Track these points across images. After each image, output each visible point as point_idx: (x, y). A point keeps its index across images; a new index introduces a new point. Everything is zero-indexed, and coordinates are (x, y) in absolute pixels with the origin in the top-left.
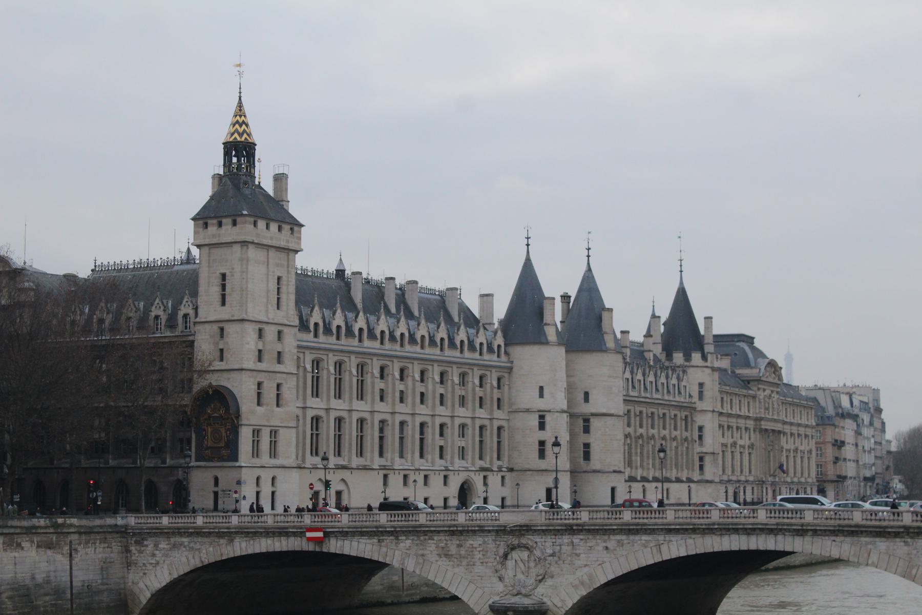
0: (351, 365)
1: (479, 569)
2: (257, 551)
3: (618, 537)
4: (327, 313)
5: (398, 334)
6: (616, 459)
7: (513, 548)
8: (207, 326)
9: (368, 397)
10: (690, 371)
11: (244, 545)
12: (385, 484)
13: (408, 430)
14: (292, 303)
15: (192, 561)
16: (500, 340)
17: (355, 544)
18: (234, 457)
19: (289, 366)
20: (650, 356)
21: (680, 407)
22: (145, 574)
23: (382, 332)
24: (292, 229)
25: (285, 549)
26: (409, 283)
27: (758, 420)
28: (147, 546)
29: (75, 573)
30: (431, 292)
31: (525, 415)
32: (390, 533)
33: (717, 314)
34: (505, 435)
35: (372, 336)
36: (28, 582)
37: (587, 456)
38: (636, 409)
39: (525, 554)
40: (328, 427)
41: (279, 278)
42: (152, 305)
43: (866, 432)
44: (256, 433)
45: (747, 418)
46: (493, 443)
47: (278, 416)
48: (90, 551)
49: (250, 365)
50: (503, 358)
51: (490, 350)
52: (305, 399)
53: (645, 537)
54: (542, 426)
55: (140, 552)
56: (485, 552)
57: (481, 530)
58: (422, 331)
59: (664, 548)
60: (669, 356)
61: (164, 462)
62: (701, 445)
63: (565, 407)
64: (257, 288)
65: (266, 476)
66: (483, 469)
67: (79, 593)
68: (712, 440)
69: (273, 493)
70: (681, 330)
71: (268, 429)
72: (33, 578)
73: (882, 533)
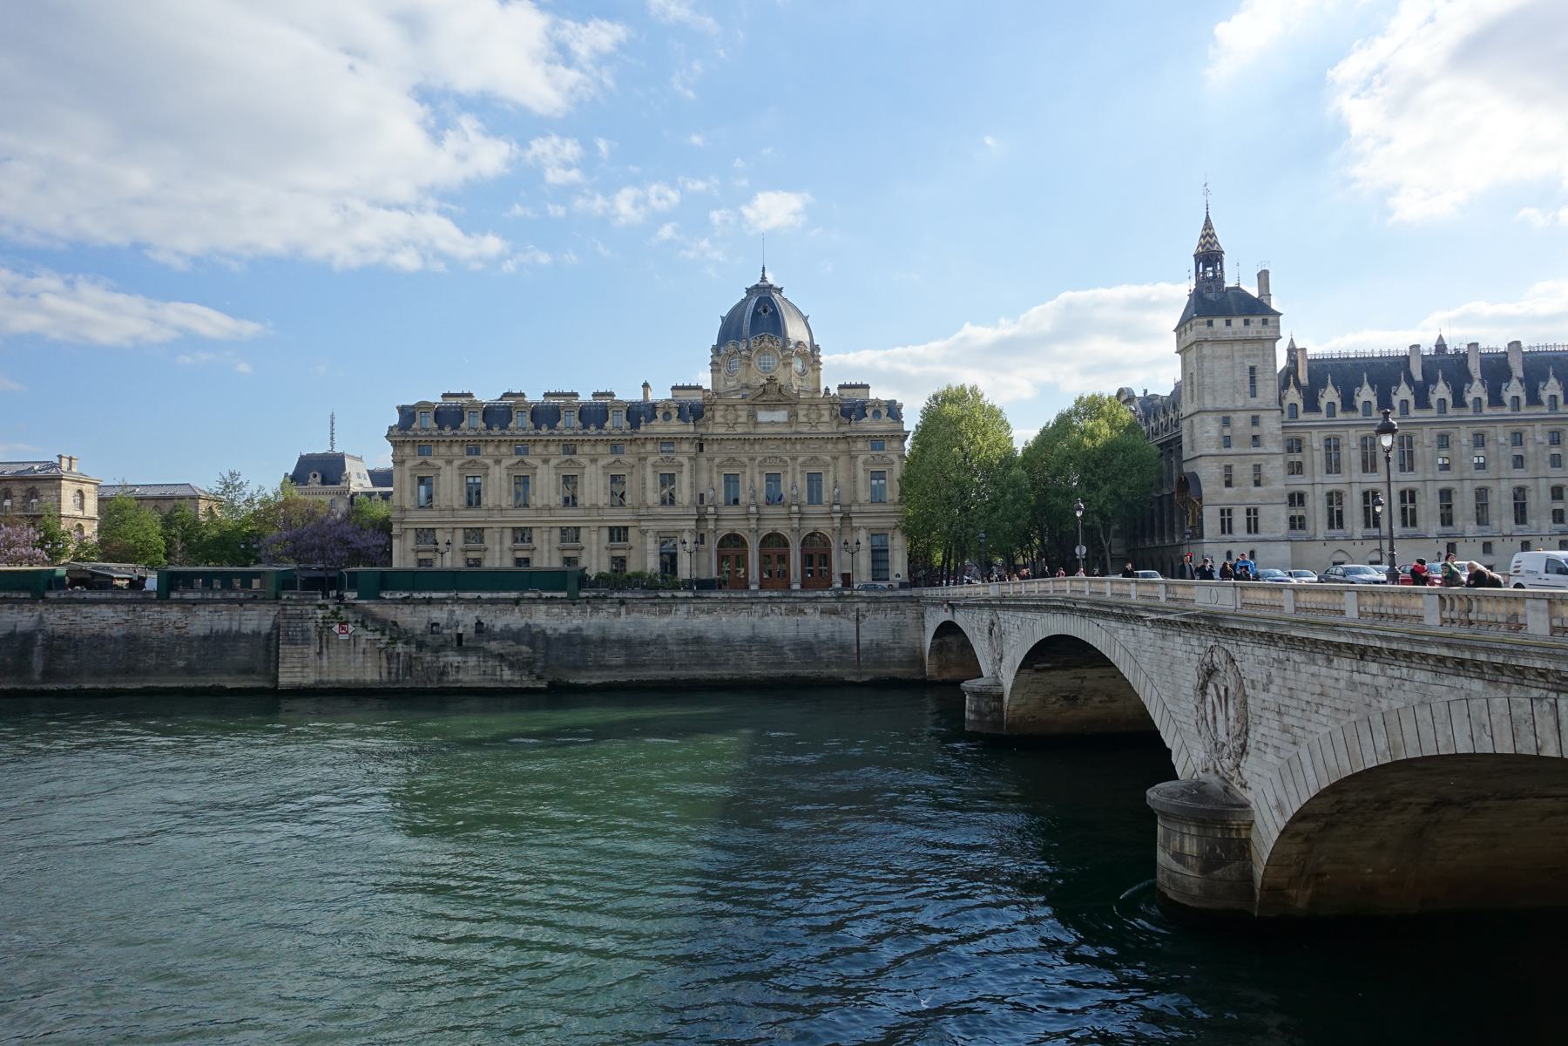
9: (1418, 467)
18: (1202, 536)
24: (1265, 322)
36: (811, 639)
41: (1252, 369)
47: (1255, 495)
48: (881, 617)
49: (1214, 451)
71: (1244, 508)
72: (816, 636)
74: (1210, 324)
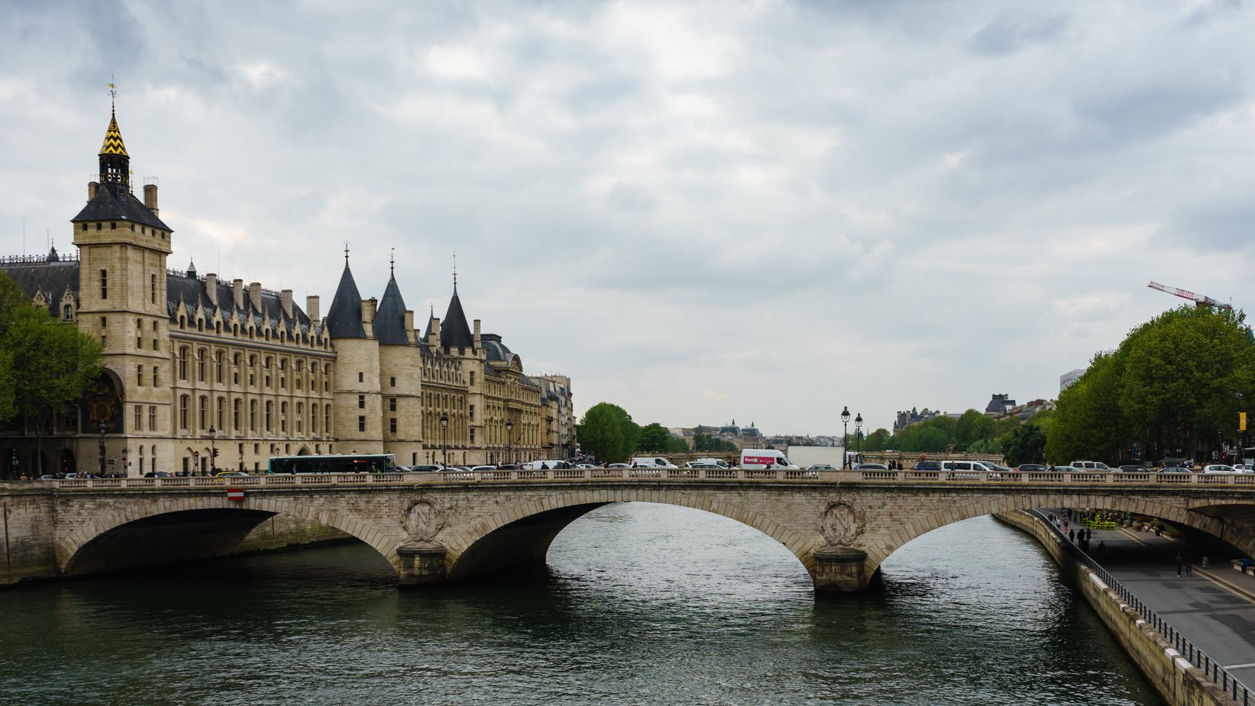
0: (212, 351)
1: (386, 521)
2: (181, 509)
3: (507, 493)
4: (189, 308)
5: (248, 327)
6: (416, 432)
7: (416, 503)
8: (89, 316)
10: (464, 362)
11: (167, 504)
12: (241, 452)
13: (258, 407)
14: (164, 298)
15: (118, 519)
16: (326, 335)
17: (273, 502)
19: (163, 352)
20: (433, 350)
21: (457, 391)
23: (218, 323)
25: (207, 507)
26: (252, 285)
27: (506, 401)
29: (10, 530)
30: (268, 292)
31: (349, 396)
32: (306, 493)
33: (482, 315)
34: (331, 411)
35: (227, 329)
37: (394, 429)
38: (431, 393)
39: (427, 508)
40: (194, 405)
42: (33, 296)
43: (564, 411)
44: (138, 408)
45: (499, 399)
46: (322, 416)
48: (22, 511)
49: (131, 350)
50: (329, 349)
51: (319, 342)
52: (175, 381)
53: (529, 493)
54: (362, 405)
56: (390, 507)
57: (388, 489)
58: (267, 325)
59: (545, 501)
60: (447, 351)
61: (51, 433)
62: (472, 420)
63: (379, 389)
64: (135, 287)
65: (148, 446)
66: (315, 440)
67: (14, 549)
68: (479, 418)
69: (153, 460)
70: (455, 328)
73: (721, 487)
74: (133, 228)
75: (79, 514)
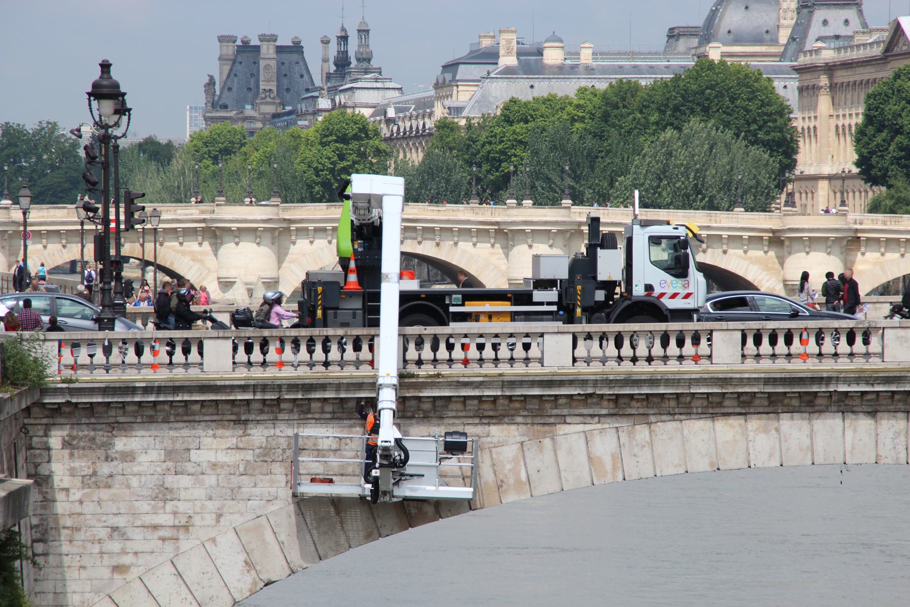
22: (118, 569)
28: (128, 457)
55: (92, 481)
75: (164, 494)
